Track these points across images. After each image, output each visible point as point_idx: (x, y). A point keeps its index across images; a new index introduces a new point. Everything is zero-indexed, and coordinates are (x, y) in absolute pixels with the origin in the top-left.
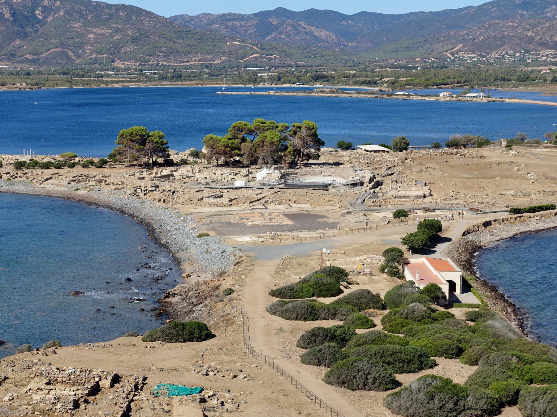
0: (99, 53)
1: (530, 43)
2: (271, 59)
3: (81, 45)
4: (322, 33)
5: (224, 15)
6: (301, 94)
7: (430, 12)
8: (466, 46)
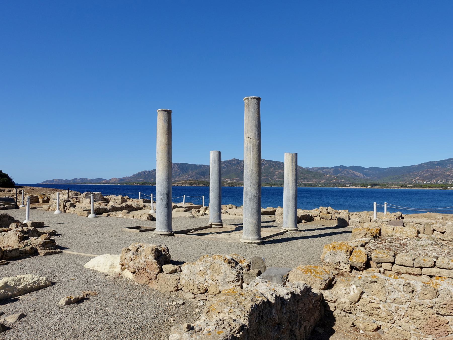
0: (279, 178)
1: (449, 177)
2: (342, 181)
3: (273, 176)
4: (358, 174)
5: (321, 168)
6: (386, 188)
7: (398, 167)
8: (421, 178)
